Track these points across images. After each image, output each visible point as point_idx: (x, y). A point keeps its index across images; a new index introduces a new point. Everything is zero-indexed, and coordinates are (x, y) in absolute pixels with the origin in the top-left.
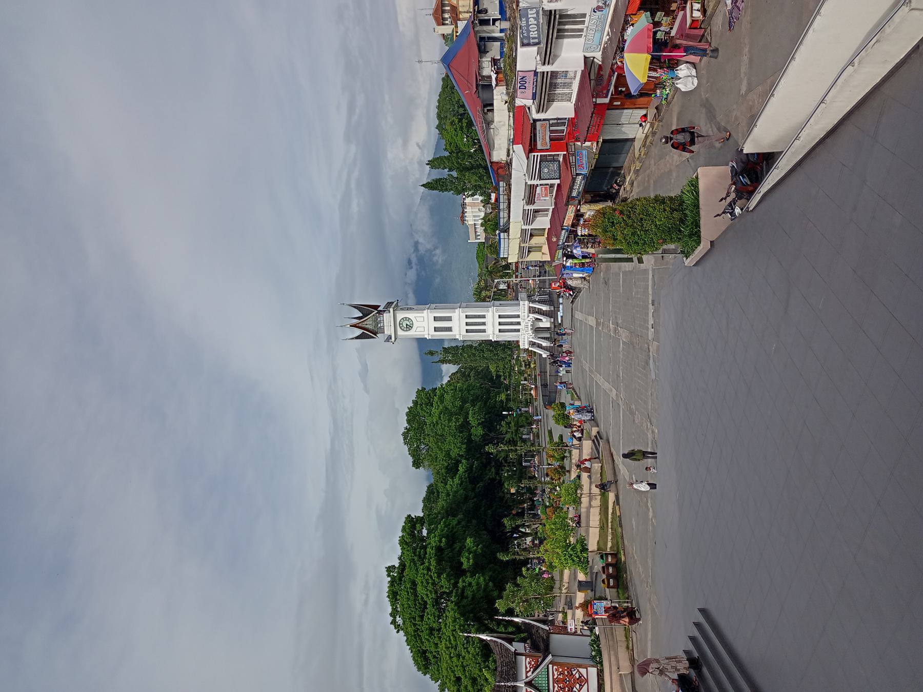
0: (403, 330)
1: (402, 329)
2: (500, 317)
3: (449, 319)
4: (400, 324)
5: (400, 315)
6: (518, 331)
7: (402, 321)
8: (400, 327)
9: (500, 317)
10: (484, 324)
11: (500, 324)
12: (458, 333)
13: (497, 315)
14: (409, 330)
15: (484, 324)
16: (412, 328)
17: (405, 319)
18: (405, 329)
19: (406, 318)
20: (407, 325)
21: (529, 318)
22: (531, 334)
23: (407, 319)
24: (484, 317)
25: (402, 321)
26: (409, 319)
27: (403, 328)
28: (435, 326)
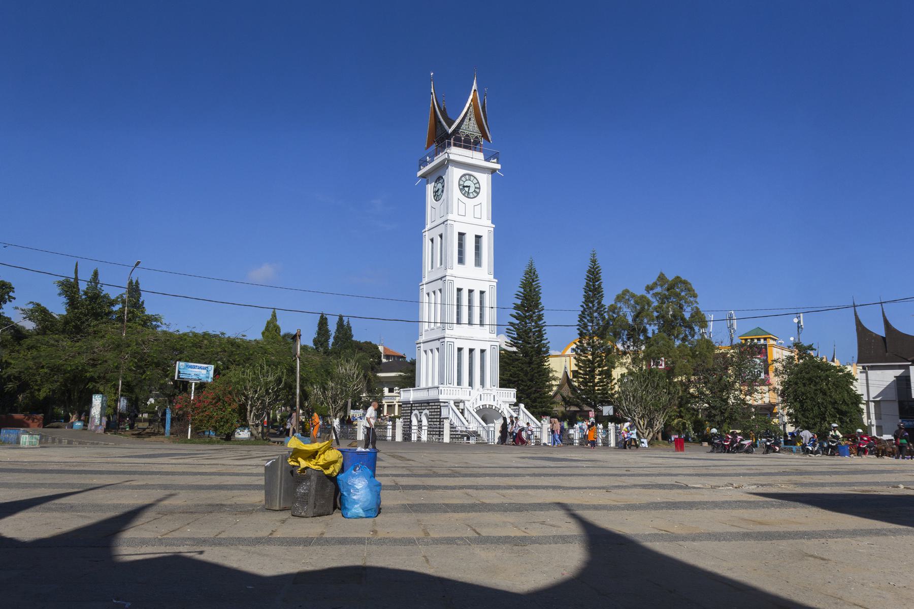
0: (460, 179)
1: (461, 177)
3: (478, 263)
4: (470, 175)
5: (485, 180)
6: (459, 383)
7: (475, 181)
8: (464, 175)
13: (486, 346)
14: (461, 190)
16: (464, 195)
17: (477, 185)
19: (479, 188)
20: (469, 187)
23: (478, 190)
25: (475, 181)
26: (478, 194)
27: (463, 179)
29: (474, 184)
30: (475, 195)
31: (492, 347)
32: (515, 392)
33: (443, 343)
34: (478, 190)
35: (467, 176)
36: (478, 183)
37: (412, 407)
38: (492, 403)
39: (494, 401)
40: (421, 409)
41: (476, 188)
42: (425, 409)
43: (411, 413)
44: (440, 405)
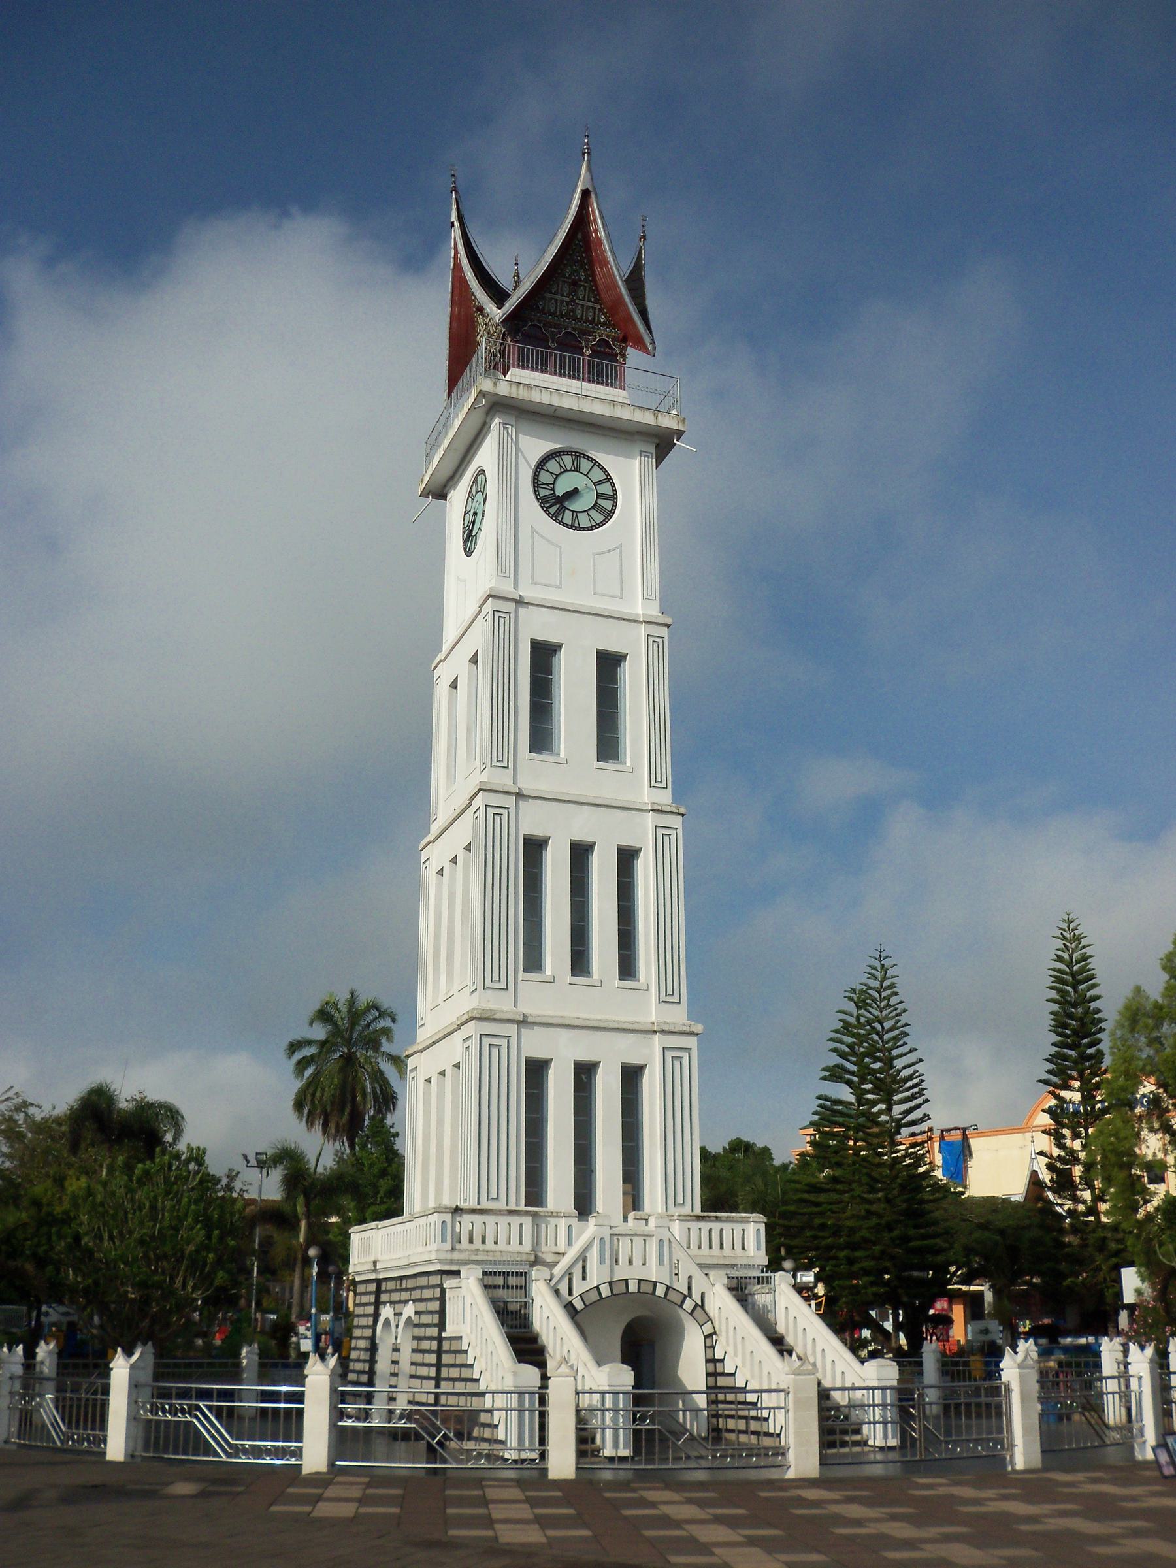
2: (631, 1076)
4: (578, 455)
9: (631, 1076)
10: (580, 962)
11: (584, 1073)
12: (526, 784)
15: (580, 962)
17: (605, 489)
18: (545, 477)
19: (613, 498)
20: (573, 494)
21: (697, 1275)
22: (579, 1287)
23: (608, 505)
24: (627, 969)
26: (609, 515)
27: (553, 466)
28: (562, 655)
29: (596, 484)
30: (599, 518)
31: (669, 1054)
32: (762, 1227)
33: (468, 1043)
34: (608, 505)
35: (568, 460)
36: (609, 479)
37: (378, 1292)
38: (653, 1272)
39: (661, 1262)
40: (400, 1302)
41: (599, 496)
42: (406, 1302)
43: (376, 1315)
44: (440, 1286)
